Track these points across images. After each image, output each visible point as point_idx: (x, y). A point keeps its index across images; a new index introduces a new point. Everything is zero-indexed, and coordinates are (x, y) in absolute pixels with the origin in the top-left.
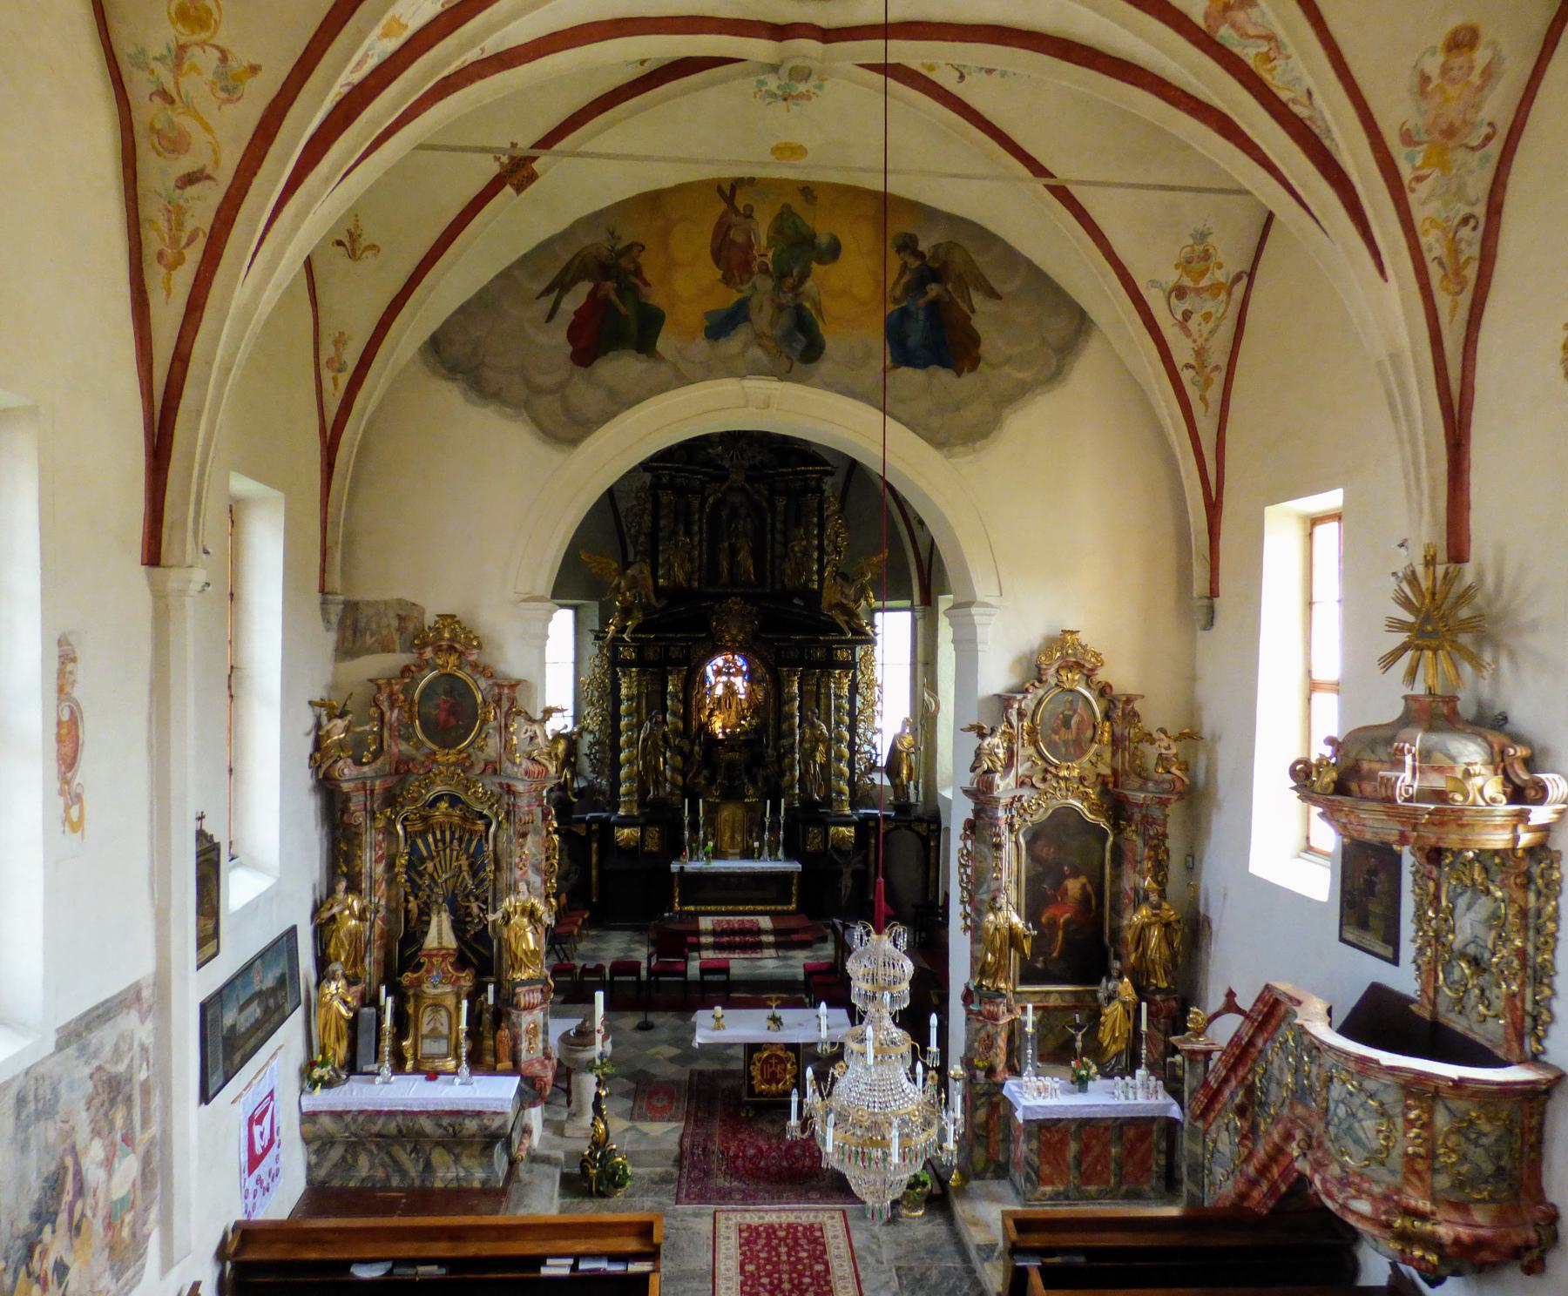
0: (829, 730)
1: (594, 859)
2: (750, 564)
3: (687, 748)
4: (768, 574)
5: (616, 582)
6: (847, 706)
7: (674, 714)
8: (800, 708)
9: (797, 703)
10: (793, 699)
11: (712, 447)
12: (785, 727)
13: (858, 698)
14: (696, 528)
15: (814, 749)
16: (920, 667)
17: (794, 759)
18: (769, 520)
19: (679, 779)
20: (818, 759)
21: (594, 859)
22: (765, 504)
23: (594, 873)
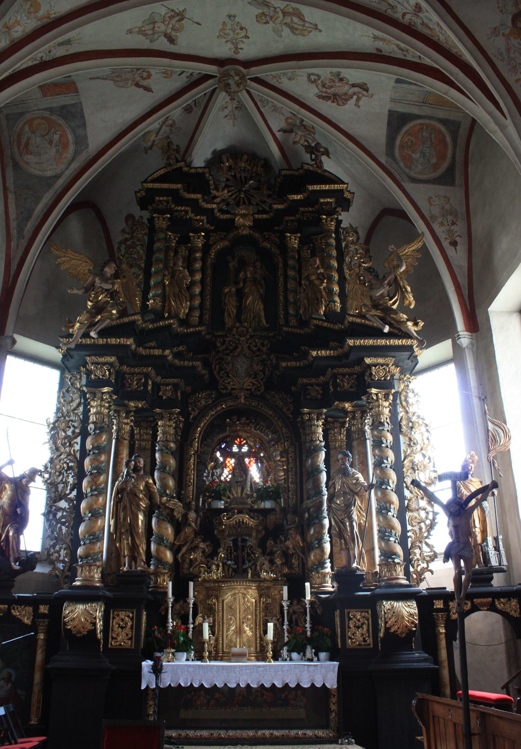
0: (367, 478)
1: (39, 657)
2: (259, 306)
3: (177, 514)
4: (281, 298)
5: (90, 279)
6: (390, 437)
7: (163, 469)
8: (327, 461)
9: (322, 455)
10: (317, 450)
11: (217, 188)
12: (309, 485)
13: (402, 438)
14: (198, 265)
15: (348, 505)
16: (476, 402)
17: (322, 526)
18: (281, 265)
19: (169, 556)
20: (355, 517)
21: (39, 657)
22: (275, 251)
23: (37, 677)
